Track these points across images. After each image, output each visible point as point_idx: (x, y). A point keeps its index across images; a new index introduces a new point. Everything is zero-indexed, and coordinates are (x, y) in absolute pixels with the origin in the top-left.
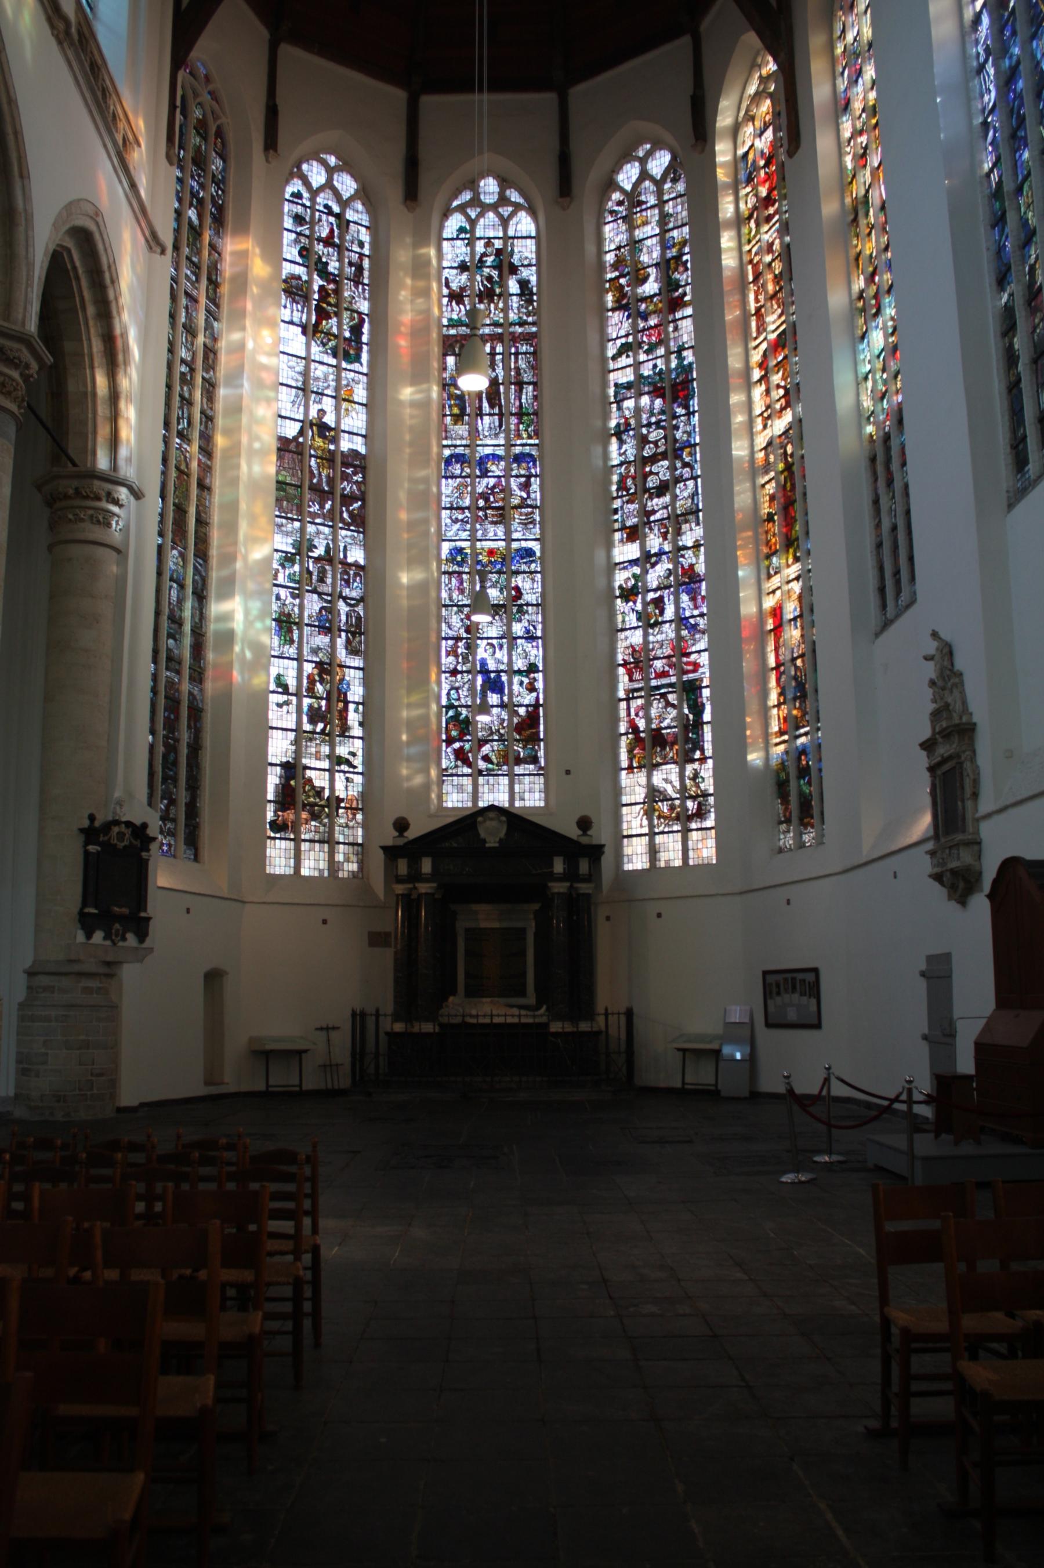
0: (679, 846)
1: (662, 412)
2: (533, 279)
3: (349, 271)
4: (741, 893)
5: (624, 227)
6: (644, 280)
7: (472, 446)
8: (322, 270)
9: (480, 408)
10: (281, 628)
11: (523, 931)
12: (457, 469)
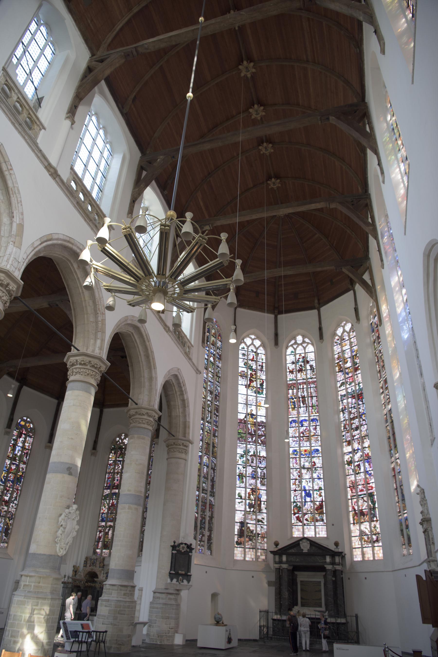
0: (371, 552)
1: (355, 403)
2: (314, 365)
3: (259, 368)
4: (392, 571)
5: (340, 347)
6: (347, 362)
7: (298, 417)
8: (251, 369)
9: (300, 405)
10: (240, 478)
11: (320, 582)
12: (294, 425)
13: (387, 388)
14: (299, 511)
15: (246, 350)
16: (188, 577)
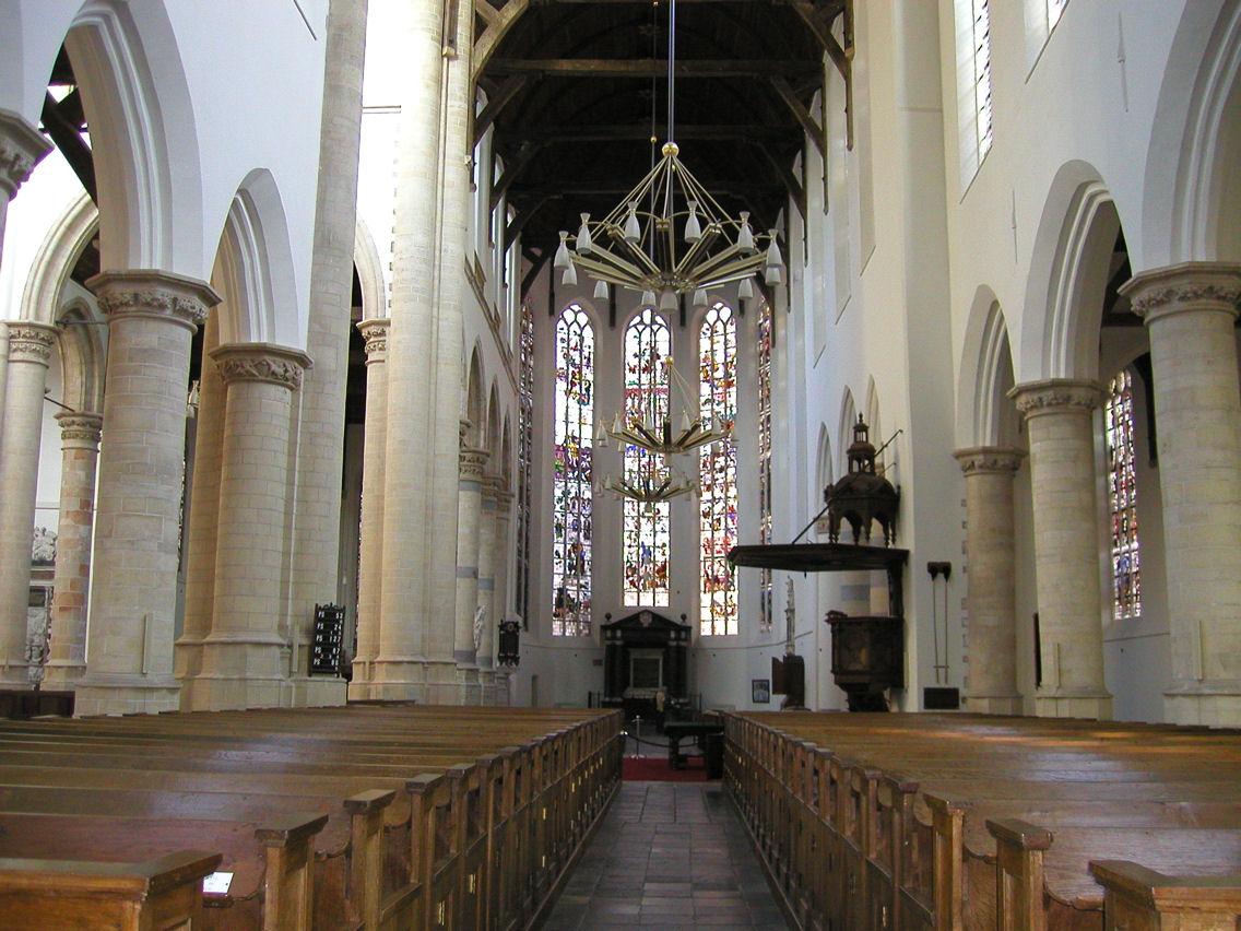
3: (585, 361)
8: (574, 365)
13: (768, 429)
16: (516, 660)
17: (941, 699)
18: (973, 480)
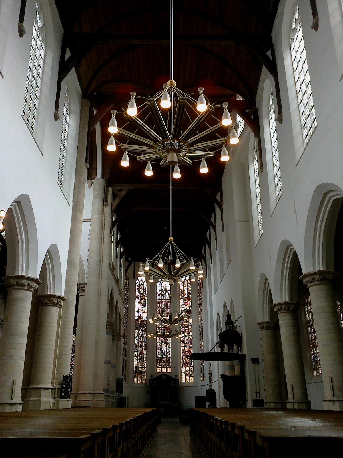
3: (144, 292)
6: (185, 295)
8: (141, 294)
13: (201, 314)
14: (160, 361)
15: (139, 283)
17: (259, 404)
18: (263, 331)
